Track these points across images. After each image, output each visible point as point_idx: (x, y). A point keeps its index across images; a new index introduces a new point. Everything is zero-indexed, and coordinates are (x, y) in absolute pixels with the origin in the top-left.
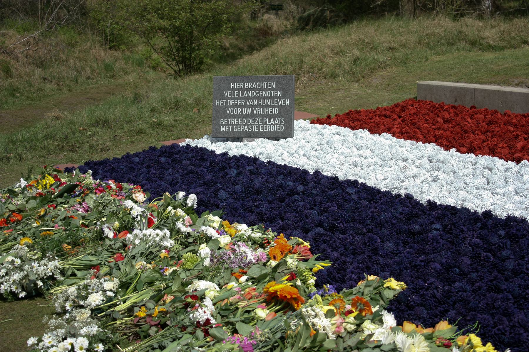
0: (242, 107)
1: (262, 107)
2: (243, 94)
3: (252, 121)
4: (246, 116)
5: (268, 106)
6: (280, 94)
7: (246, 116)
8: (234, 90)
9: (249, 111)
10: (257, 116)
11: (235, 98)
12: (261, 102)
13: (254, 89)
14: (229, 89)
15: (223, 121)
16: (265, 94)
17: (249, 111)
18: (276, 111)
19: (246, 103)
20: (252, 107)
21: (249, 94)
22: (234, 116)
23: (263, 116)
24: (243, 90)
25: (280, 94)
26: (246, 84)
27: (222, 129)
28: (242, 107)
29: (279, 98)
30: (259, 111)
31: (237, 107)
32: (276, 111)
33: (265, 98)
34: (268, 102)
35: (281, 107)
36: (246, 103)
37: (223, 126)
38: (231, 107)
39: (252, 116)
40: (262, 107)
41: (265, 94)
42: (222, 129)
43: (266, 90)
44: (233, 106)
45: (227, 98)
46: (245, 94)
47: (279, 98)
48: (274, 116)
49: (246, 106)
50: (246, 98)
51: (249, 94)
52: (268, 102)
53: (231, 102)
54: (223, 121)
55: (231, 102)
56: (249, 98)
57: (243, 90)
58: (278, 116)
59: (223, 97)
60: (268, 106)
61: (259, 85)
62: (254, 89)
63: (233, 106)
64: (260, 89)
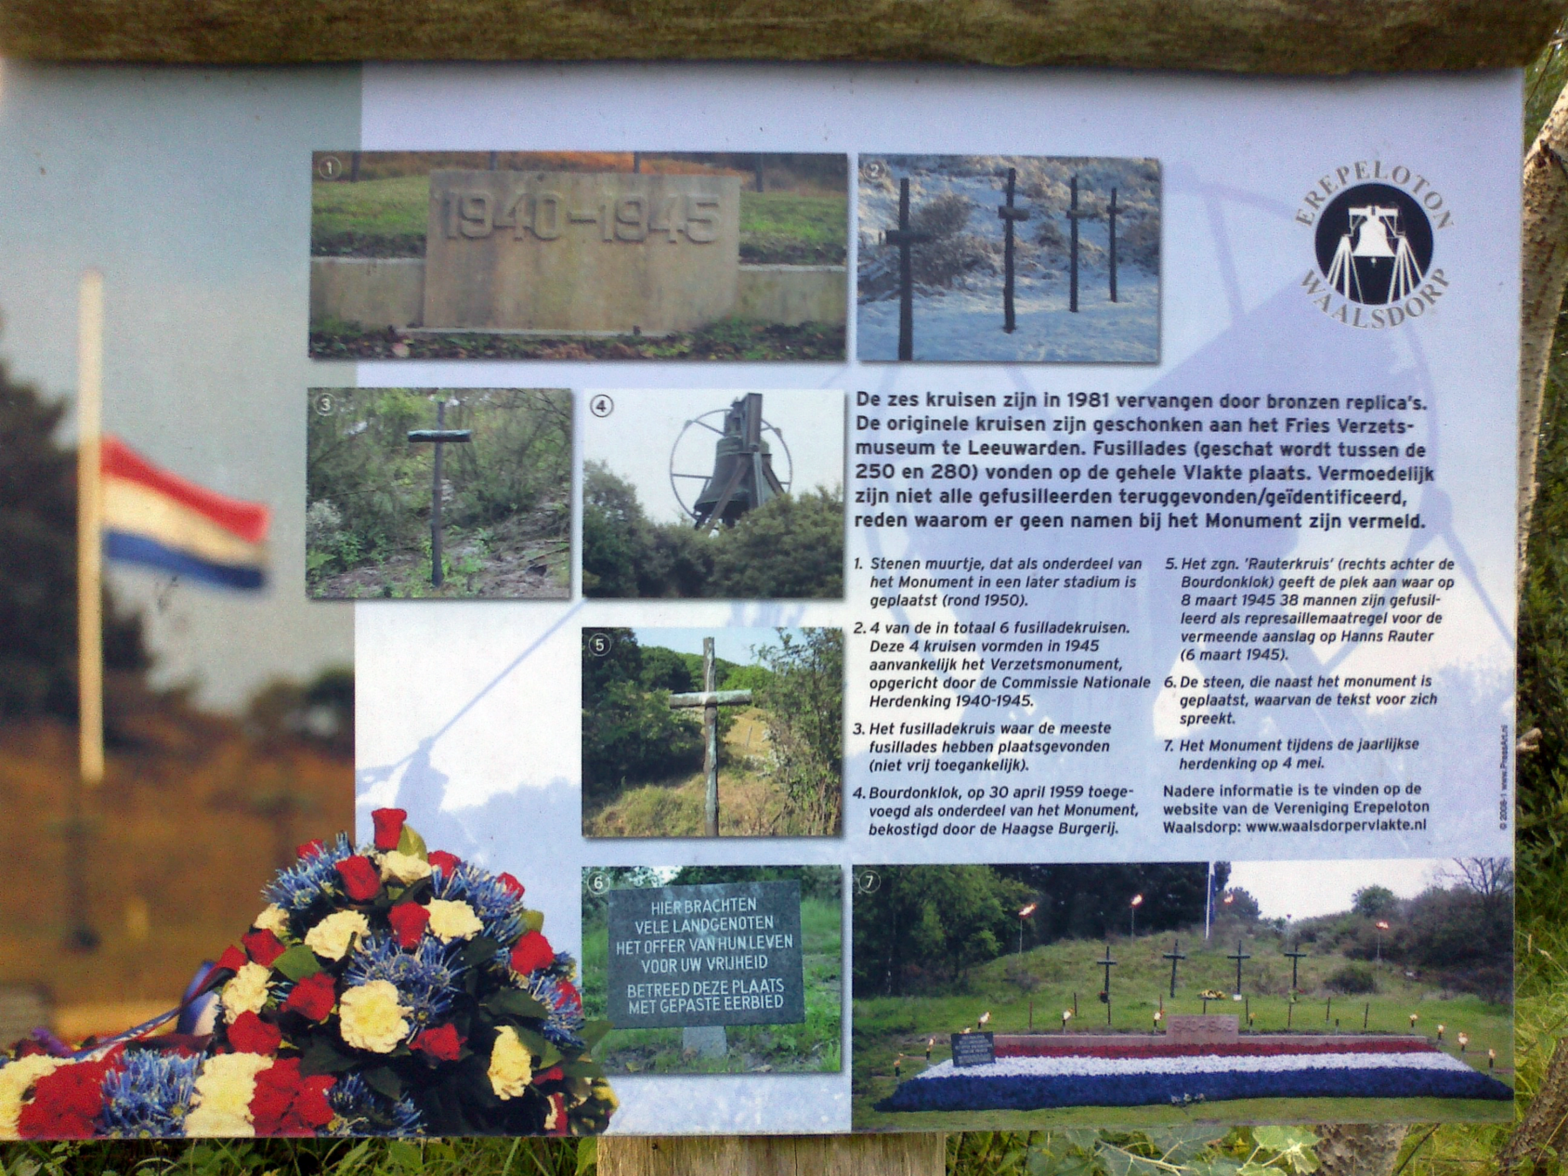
0: (678, 956)
2: (679, 927)
3: (703, 986)
4: (691, 976)
6: (769, 922)
7: (691, 976)
8: (659, 918)
10: (717, 974)
11: (660, 937)
15: (631, 990)
16: (733, 924)
17: (696, 965)
19: (687, 946)
22: (661, 978)
23: (730, 975)
25: (769, 922)
27: (633, 1008)
28: (678, 956)
31: (666, 955)
34: (741, 942)
36: (687, 946)
37: (634, 1001)
38: (652, 956)
39: (705, 974)
42: (633, 1008)
45: (643, 938)
47: (768, 932)
48: (759, 975)
49: (689, 953)
52: (741, 942)
54: (631, 990)
58: (770, 972)
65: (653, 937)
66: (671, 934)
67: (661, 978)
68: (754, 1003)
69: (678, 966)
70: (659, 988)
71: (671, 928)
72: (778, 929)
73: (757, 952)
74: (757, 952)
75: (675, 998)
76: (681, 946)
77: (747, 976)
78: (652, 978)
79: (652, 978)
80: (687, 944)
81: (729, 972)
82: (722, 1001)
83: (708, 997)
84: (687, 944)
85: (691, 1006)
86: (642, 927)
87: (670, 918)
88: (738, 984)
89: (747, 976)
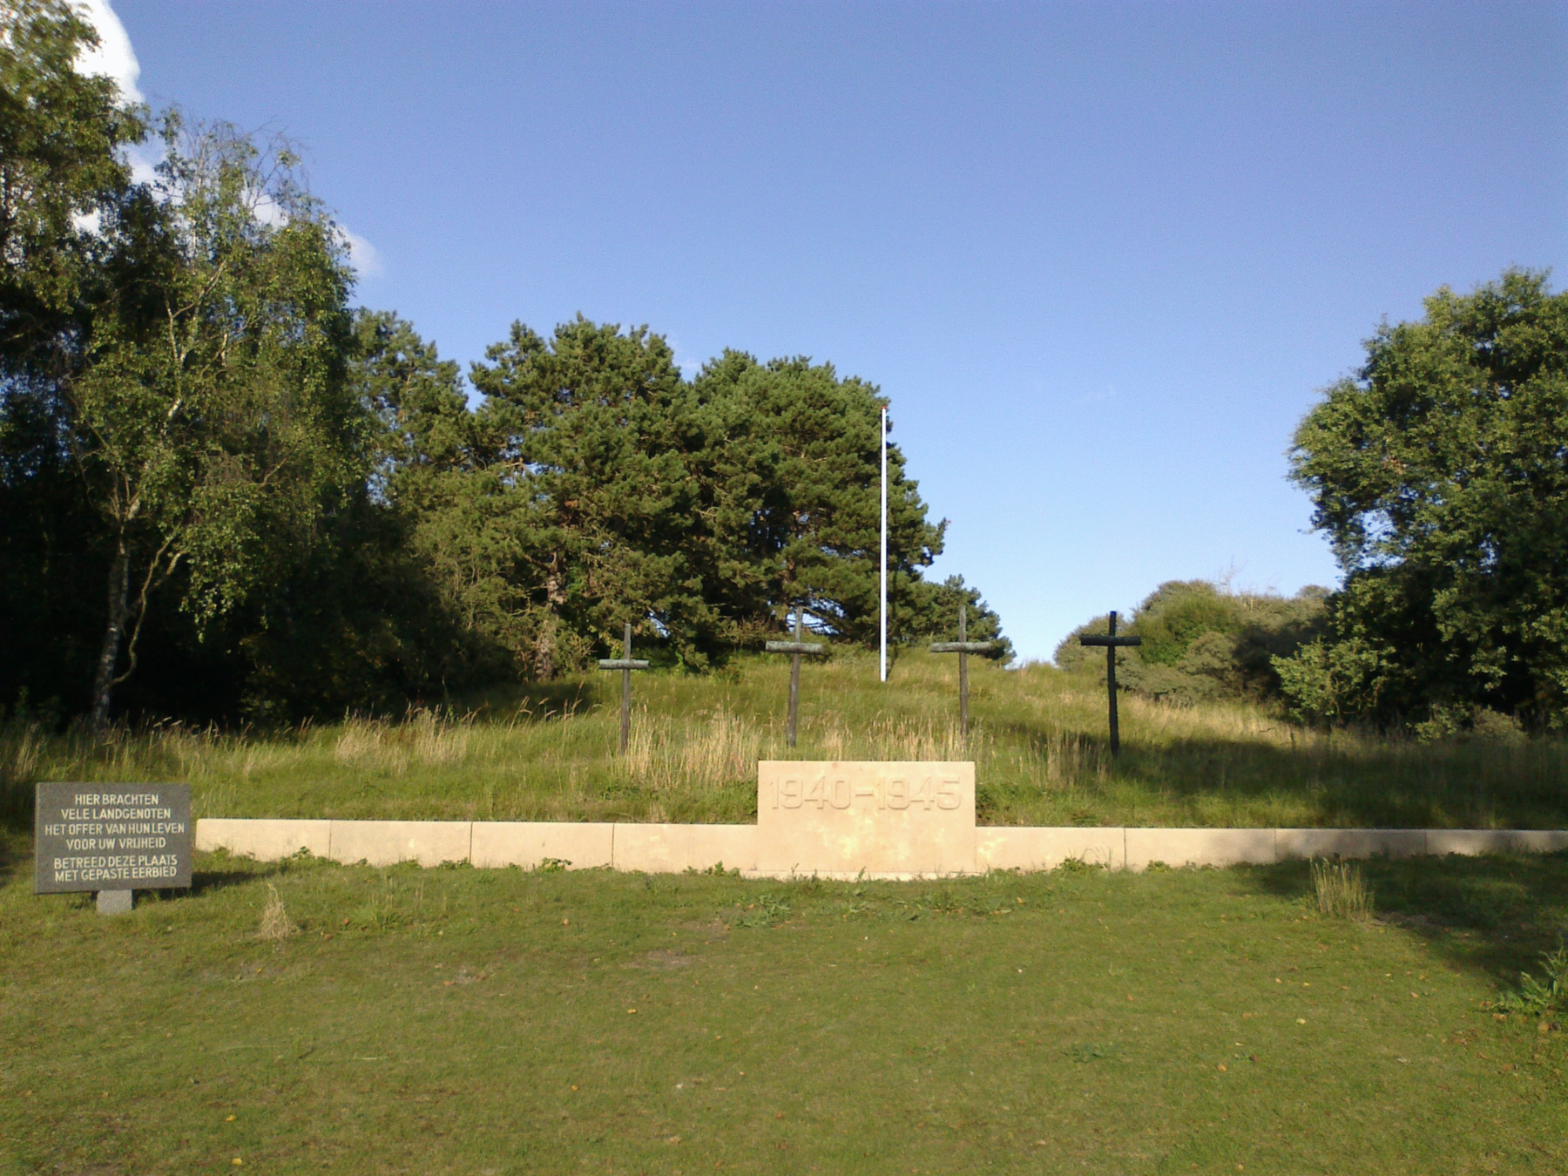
0: (96, 837)
1: (135, 836)
2: (98, 814)
3: (116, 860)
4: (106, 853)
5: (146, 835)
6: (167, 813)
7: (106, 853)
8: (81, 807)
9: (111, 844)
10: (127, 851)
11: (82, 822)
12: (133, 828)
13: (120, 806)
14: (70, 804)
15: (57, 863)
16: (140, 814)
17: (111, 844)
18: (161, 843)
19: (104, 829)
20: (115, 836)
21: (111, 814)
22: (82, 854)
23: (138, 852)
24: (99, 808)
25: (167, 813)
26: (105, 797)
27: (58, 877)
28: (96, 837)
29: (166, 821)
31: (87, 835)
32: (161, 843)
33: (140, 821)
34: (146, 828)
35: (169, 836)
36: (104, 829)
37: (60, 871)
38: (75, 837)
39: (117, 851)
40: (135, 836)
41: (140, 814)
42: (58, 877)
43: (142, 807)
44: (80, 836)
45: (68, 822)
46: (103, 814)
47: (166, 821)
48: (158, 852)
49: (105, 835)
50: (104, 821)
51: (111, 814)
52: (146, 828)
53: (75, 829)
54: (57, 863)
55: (75, 829)
56: (110, 821)
57: (99, 808)
59: (60, 820)
60: (146, 835)
62: (120, 806)
63: (80, 836)
65: (75, 822)
66: (91, 821)
67: (82, 854)
68: (155, 873)
70: (79, 861)
72: (174, 819)
73: (158, 835)
75: (93, 871)
76: (99, 829)
77: (150, 853)
78: (75, 853)
79: (75, 853)
82: (130, 870)
83: (117, 868)
85: (106, 875)
86: (67, 814)
89: (150, 853)
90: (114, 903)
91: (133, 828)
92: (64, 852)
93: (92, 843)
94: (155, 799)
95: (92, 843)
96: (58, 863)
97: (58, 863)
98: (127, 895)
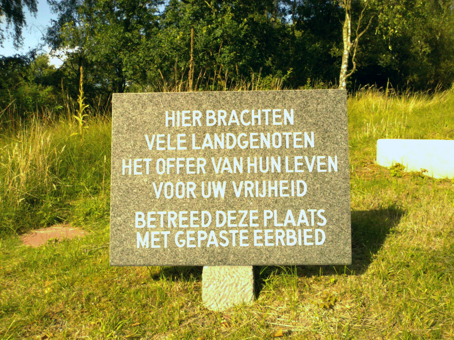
2: (199, 142)
3: (228, 216)
4: (212, 204)
5: (276, 176)
6: (310, 140)
11: (175, 154)
12: (253, 164)
16: (266, 141)
17: (219, 190)
19: (210, 168)
20: (227, 177)
22: (175, 205)
23: (262, 204)
24: (200, 132)
25: (310, 140)
28: (196, 178)
29: (309, 152)
30: (248, 188)
33: (265, 153)
34: (275, 164)
36: (210, 168)
37: (144, 231)
39: (231, 202)
41: (266, 141)
42: (142, 242)
47: (309, 152)
49: (210, 175)
52: (275, 164)
57: (200, 132)
58: (310, 201)
59: (141, 152)
61: (247, 118)
64: (250, 129)
65: (167, 154)
69: (198, 191)
71: (188, 145)
72: (321, 148)
73: (294, 176)
74: (294, 176)
77: (282, 205)
80: (209, 164)
81: (259, 200)
84: (209, 164)
85: (213, 240)
86: (153, 141)
87: (187, 131)
88: (271, 214)
89: (282, 205)
90: (225, 289)
91: (253, 164)
92: (148, 201)
93: (190, 188)
94: (289, 116)
95: (190, 188)
96: (140, 219)
97: (140, 219)
98: (246, 275)
